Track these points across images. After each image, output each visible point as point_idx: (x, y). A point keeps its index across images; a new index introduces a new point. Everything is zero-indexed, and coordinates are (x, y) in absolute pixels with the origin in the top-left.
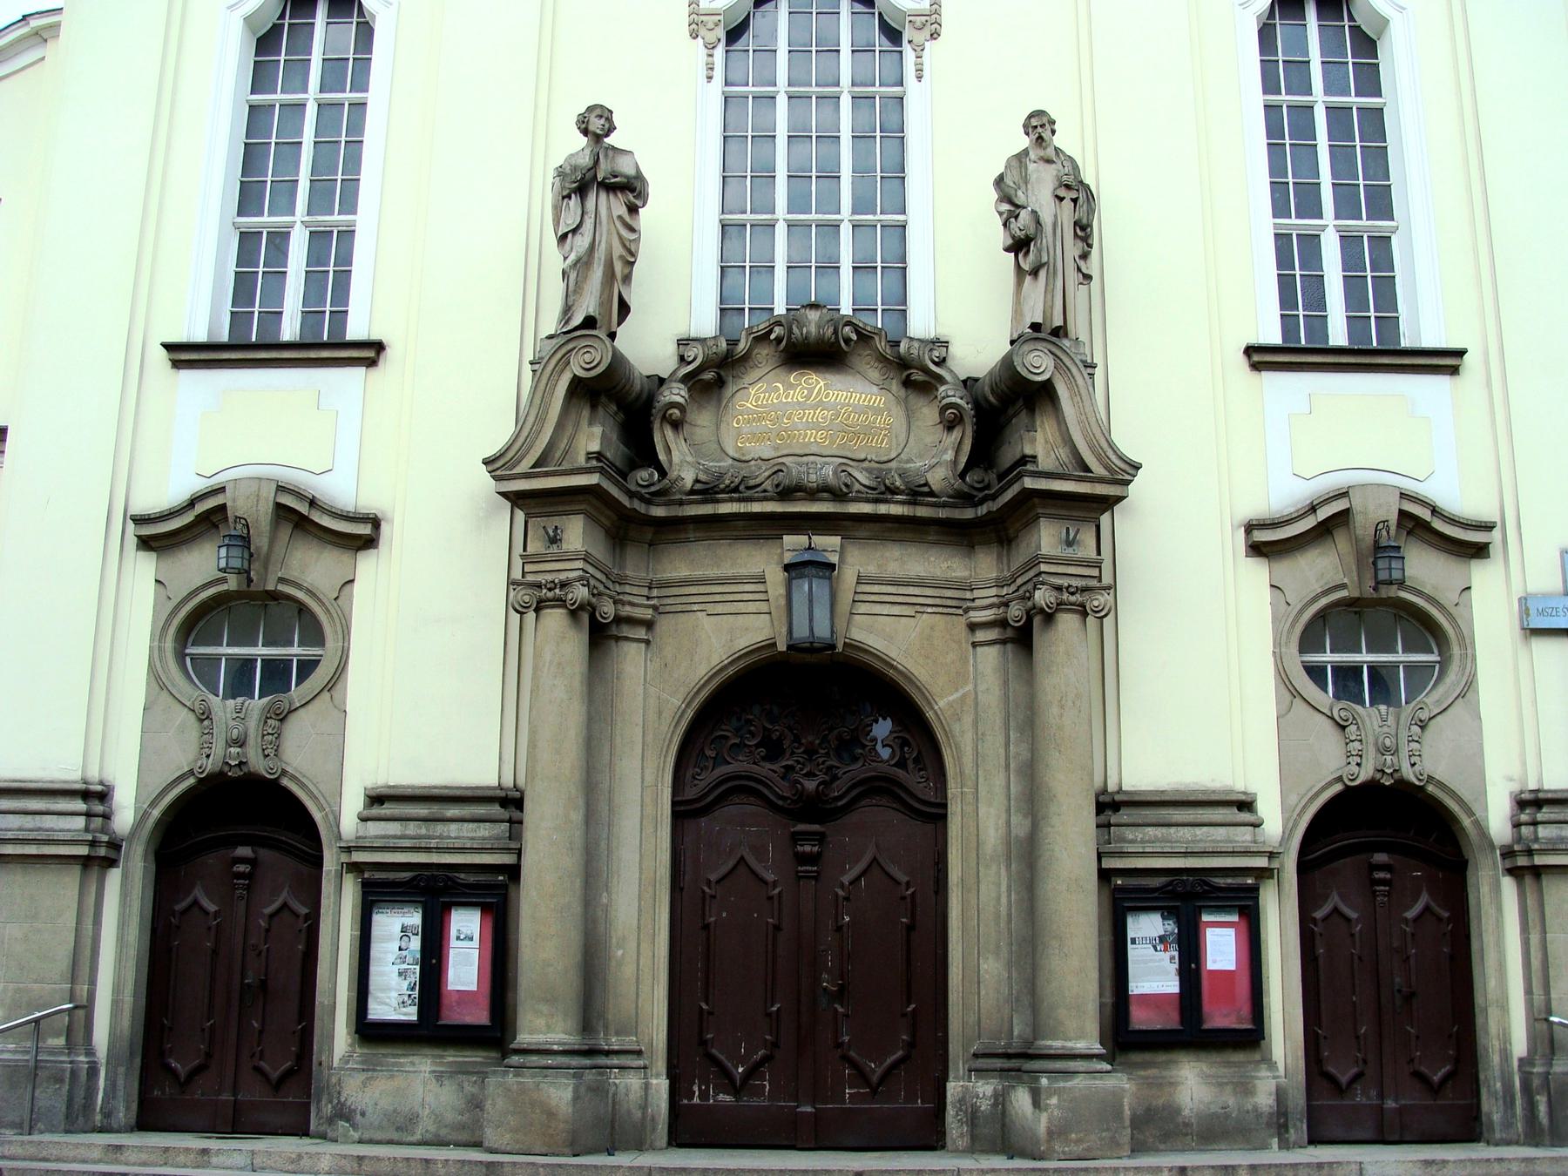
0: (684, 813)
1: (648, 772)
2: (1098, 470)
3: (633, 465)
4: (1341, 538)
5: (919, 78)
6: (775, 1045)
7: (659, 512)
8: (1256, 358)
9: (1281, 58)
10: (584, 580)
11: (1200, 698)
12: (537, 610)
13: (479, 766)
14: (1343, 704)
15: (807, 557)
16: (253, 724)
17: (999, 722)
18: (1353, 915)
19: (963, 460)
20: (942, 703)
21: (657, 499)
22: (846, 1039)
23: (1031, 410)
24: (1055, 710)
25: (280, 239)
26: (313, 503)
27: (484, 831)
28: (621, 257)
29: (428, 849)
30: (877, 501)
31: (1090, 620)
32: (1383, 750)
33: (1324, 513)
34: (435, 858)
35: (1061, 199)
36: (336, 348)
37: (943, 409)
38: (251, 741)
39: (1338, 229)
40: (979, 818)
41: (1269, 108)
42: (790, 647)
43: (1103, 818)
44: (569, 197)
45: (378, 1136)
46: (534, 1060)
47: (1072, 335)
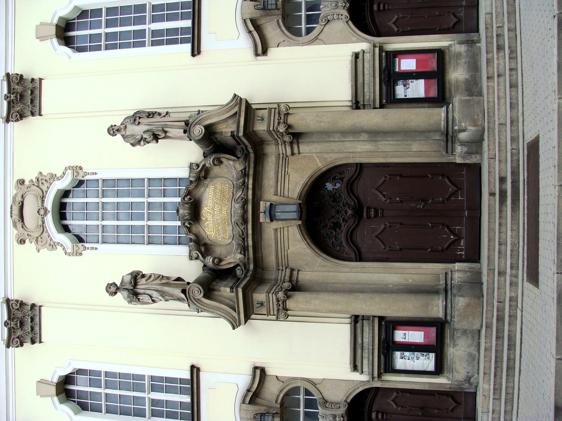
0: (360, 258)
1: (345, 271)
2: (236, 109)
3: (235, 276)
4: (260, 22)
5: (96, 174)
6: (443, 225)
7: (252, 267)
8: (196, 53)
9: (88, 44)
10: (276, 293)
12: (287, 310)
13: (342, 332)
14: (320, 21)
15: (268, 213)
16: (328, 412)
17: (327, 145)
18: (396, 17)
19: (232, 157)
20: (320, 165)
21: (247, 267)
22: (441, 199)
23: (215, 133)
24: (323, 124)
25: (154, 402)
26: (248, 391)
27: (366, 329)
28: (160, 280)
29: (373, 349)
30: (248, 189)
31: (290, 112)
32: (337, 6)
33: (252, 28)
34: (376, 347)
35: (139, 123)
36: (193, 382)
37: (215, 165)
38: (334, 413)
39: (150, 23)
40: (361, 151)
41: (106, 49)
42: (300, 219)
43: (361, 107)
45: (476, 367)
46: (449, 311)
47: (188, 119)
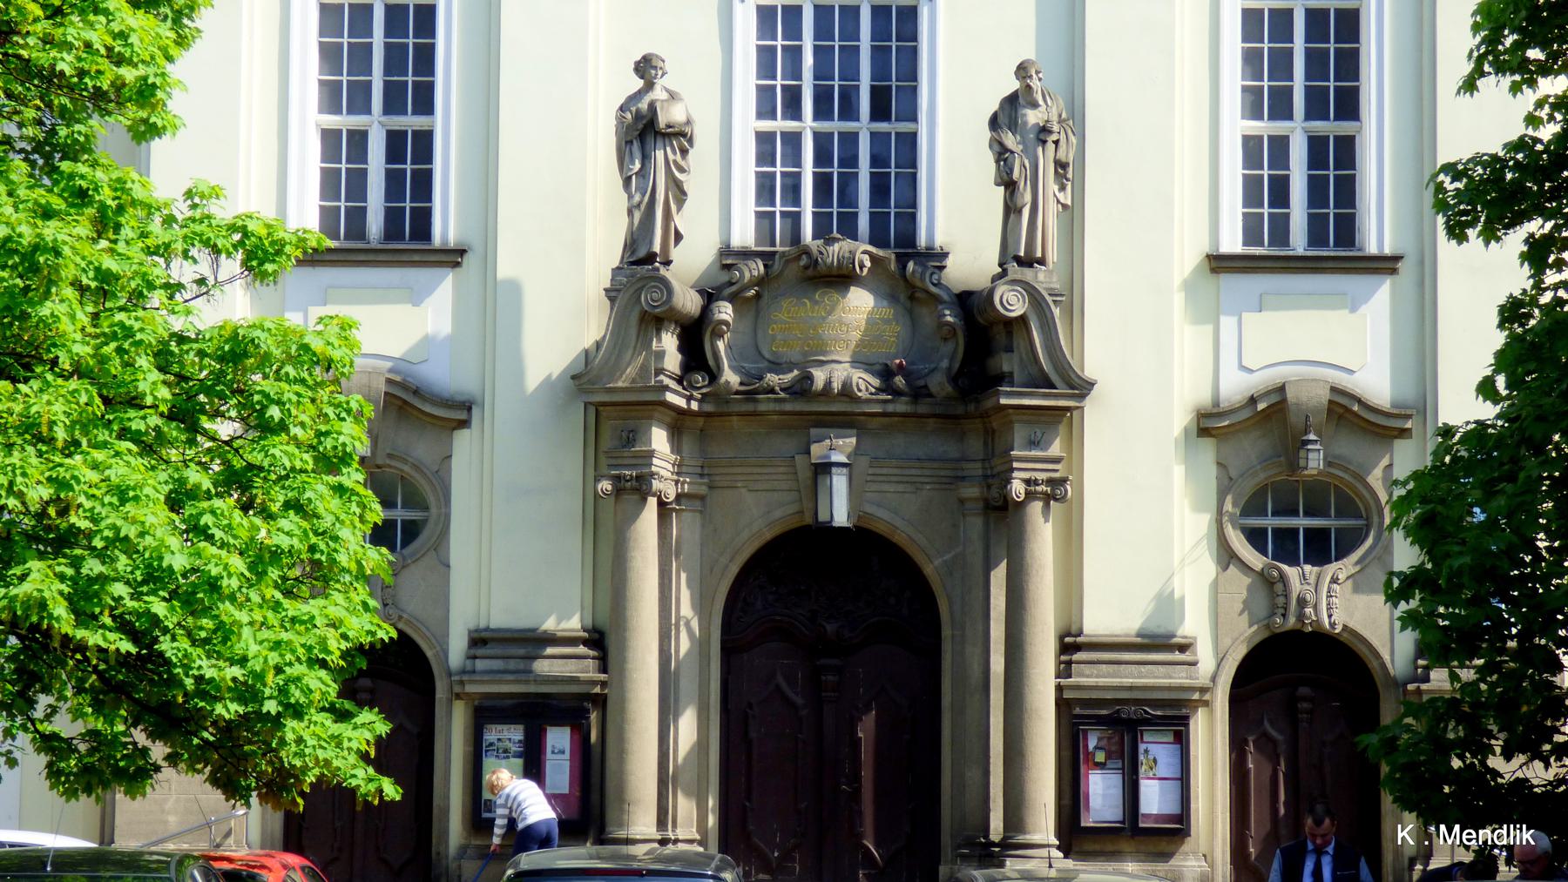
19: (957, 365)
26: (416, 392)
44: (631, 142)
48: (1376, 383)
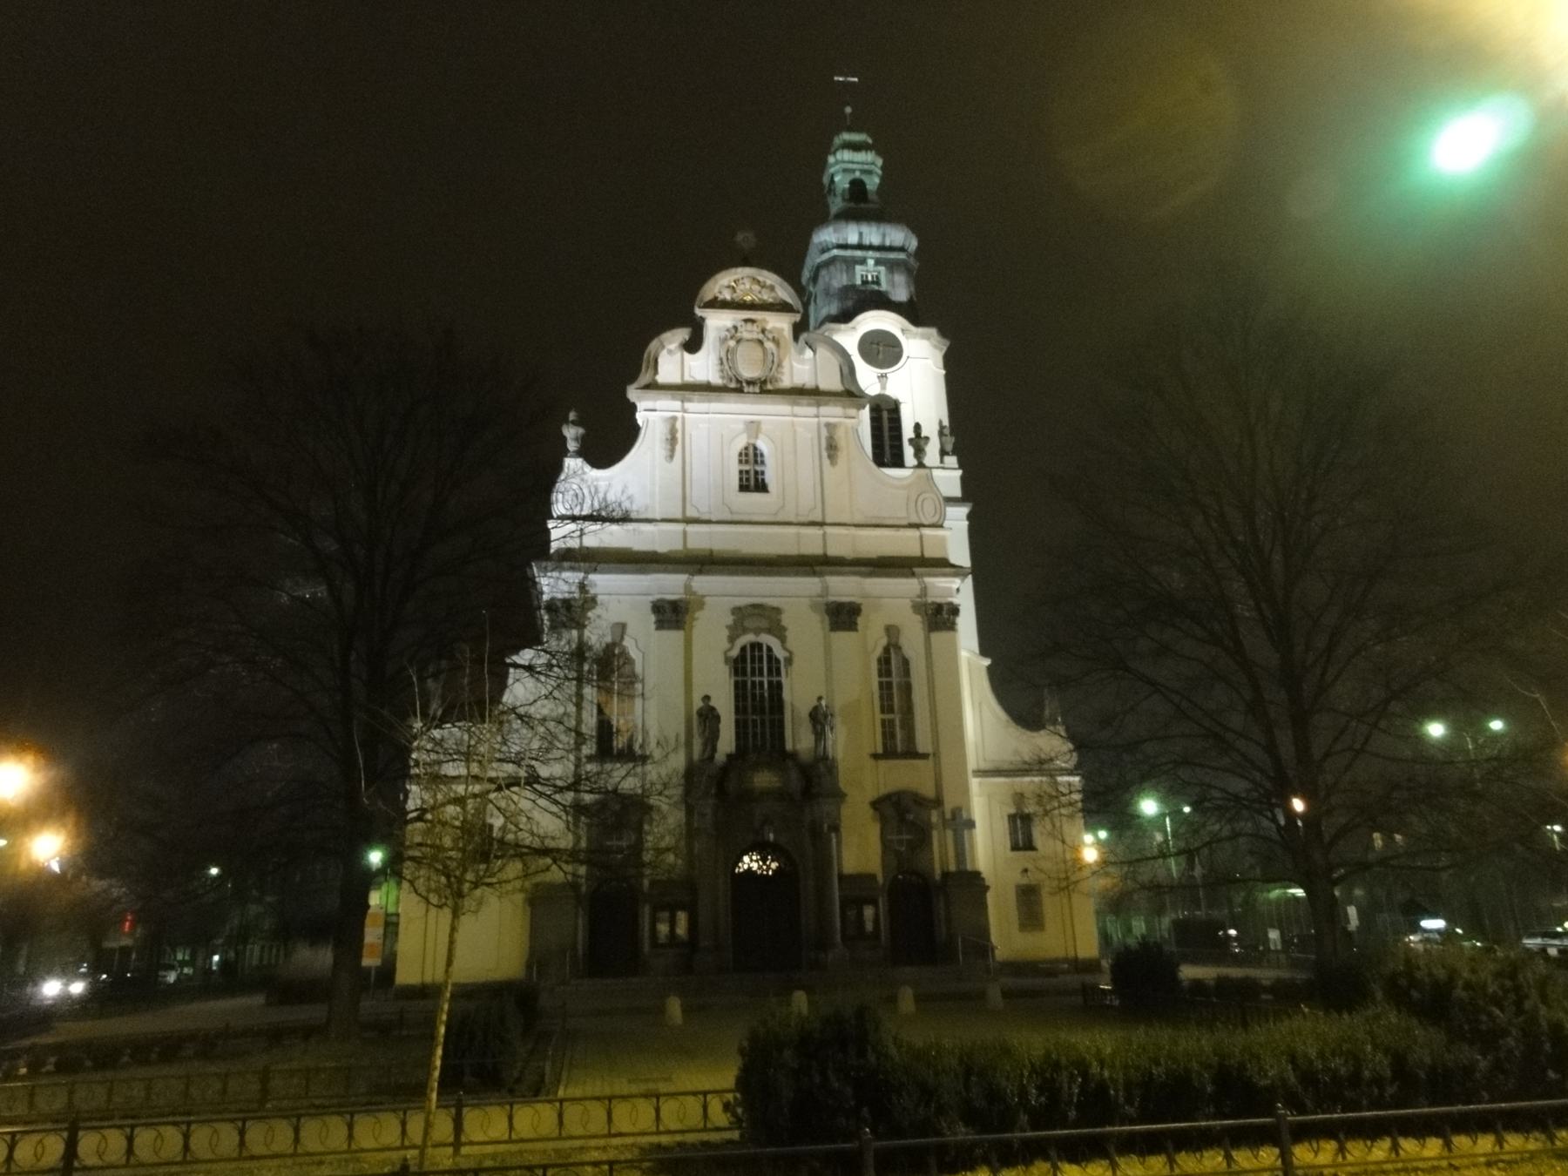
11: (860, 849)
48: (928, 791)
